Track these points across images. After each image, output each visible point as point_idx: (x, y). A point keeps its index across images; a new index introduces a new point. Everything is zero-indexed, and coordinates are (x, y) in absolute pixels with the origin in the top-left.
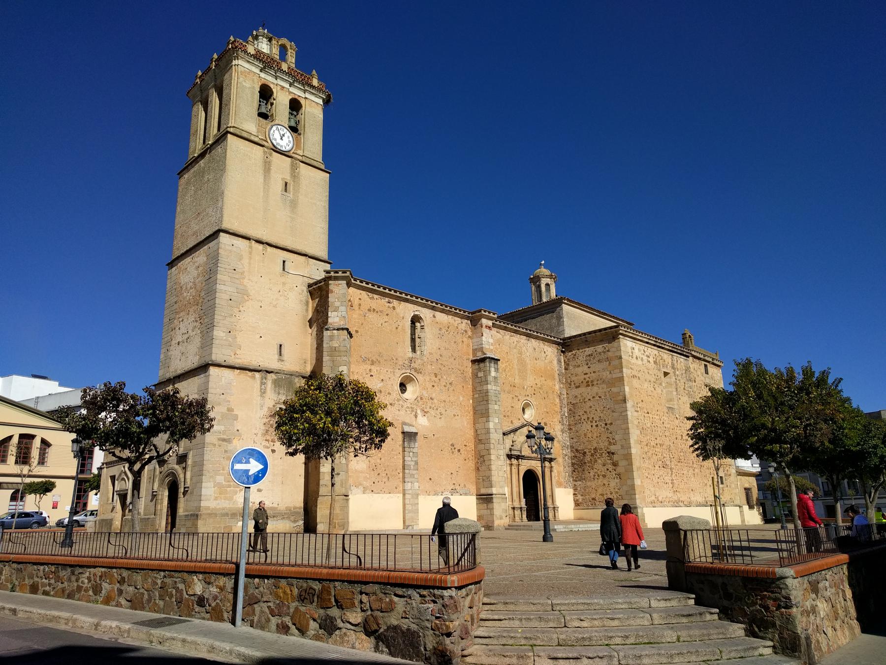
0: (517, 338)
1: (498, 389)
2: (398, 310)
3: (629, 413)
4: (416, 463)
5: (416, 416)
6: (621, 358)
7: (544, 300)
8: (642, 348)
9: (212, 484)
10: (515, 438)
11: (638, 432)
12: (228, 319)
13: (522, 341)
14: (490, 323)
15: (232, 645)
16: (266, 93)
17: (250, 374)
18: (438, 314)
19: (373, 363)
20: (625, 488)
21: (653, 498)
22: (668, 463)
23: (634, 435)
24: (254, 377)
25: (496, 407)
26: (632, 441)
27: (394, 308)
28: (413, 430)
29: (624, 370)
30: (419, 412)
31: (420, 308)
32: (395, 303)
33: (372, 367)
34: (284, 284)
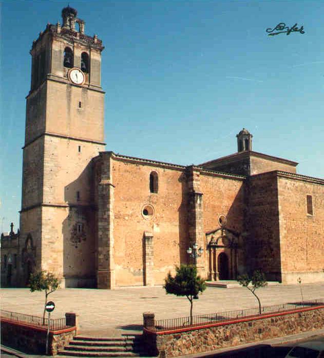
0: (216, 179)
1: (202, 210)
2: (142, 170)
3: (280, 221)
4: (152, 252)
5: (153, 227)
6: (277, 189)
7: (194, 172)
8: (293, 182)
9: (46, 263)
10: (214, 236)
11: (286, 232)
12: (50, 181)
13: (220, 180)
14: (198, 173)
15: (166, 267)
16: (69, 53)
17: (63, 208)
18: (166, 169)
19: (128, 200)
20: (276, 263)
21: (293, 268)
22: (305, 248)
23: (283, 233)
24: (65, 210)
25: (200, 221)
26: (281, 237)
27: (140, 169)
28: (151, 235)
29: (279, 197)
30: (155, 224)
31: (155, 168)
32: (141, 166)
33: (127, 203)
34: (80, 159)
